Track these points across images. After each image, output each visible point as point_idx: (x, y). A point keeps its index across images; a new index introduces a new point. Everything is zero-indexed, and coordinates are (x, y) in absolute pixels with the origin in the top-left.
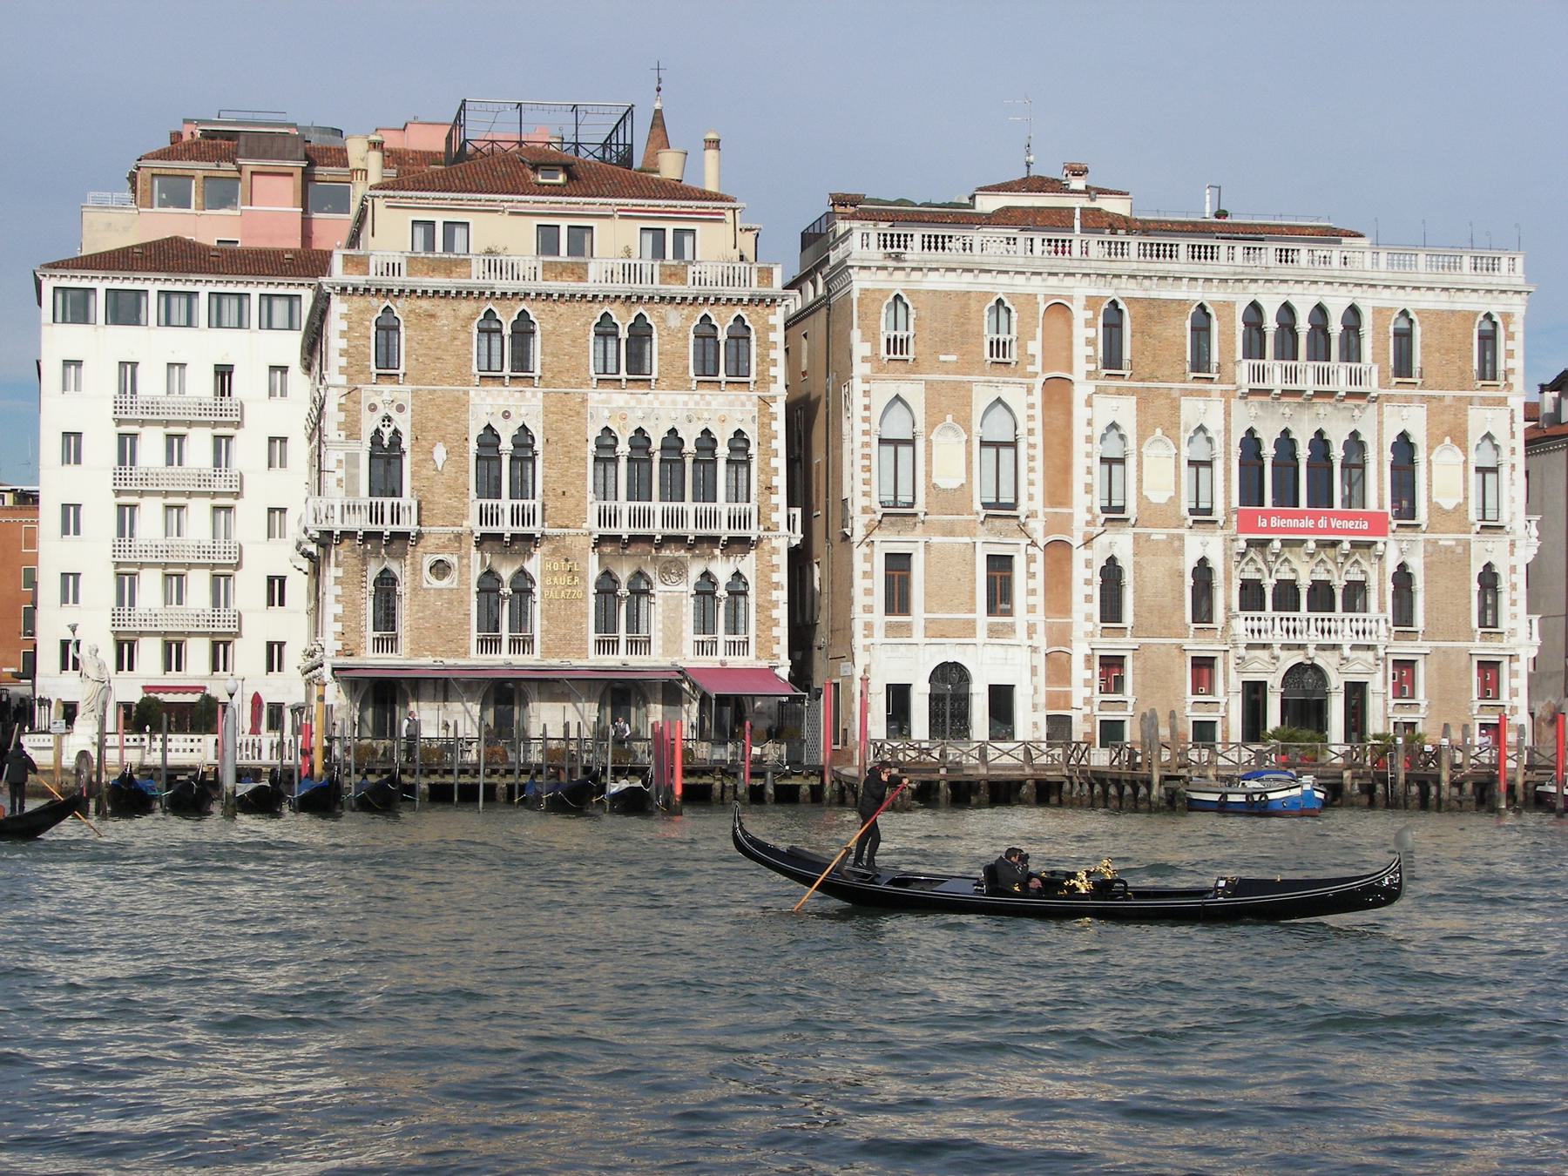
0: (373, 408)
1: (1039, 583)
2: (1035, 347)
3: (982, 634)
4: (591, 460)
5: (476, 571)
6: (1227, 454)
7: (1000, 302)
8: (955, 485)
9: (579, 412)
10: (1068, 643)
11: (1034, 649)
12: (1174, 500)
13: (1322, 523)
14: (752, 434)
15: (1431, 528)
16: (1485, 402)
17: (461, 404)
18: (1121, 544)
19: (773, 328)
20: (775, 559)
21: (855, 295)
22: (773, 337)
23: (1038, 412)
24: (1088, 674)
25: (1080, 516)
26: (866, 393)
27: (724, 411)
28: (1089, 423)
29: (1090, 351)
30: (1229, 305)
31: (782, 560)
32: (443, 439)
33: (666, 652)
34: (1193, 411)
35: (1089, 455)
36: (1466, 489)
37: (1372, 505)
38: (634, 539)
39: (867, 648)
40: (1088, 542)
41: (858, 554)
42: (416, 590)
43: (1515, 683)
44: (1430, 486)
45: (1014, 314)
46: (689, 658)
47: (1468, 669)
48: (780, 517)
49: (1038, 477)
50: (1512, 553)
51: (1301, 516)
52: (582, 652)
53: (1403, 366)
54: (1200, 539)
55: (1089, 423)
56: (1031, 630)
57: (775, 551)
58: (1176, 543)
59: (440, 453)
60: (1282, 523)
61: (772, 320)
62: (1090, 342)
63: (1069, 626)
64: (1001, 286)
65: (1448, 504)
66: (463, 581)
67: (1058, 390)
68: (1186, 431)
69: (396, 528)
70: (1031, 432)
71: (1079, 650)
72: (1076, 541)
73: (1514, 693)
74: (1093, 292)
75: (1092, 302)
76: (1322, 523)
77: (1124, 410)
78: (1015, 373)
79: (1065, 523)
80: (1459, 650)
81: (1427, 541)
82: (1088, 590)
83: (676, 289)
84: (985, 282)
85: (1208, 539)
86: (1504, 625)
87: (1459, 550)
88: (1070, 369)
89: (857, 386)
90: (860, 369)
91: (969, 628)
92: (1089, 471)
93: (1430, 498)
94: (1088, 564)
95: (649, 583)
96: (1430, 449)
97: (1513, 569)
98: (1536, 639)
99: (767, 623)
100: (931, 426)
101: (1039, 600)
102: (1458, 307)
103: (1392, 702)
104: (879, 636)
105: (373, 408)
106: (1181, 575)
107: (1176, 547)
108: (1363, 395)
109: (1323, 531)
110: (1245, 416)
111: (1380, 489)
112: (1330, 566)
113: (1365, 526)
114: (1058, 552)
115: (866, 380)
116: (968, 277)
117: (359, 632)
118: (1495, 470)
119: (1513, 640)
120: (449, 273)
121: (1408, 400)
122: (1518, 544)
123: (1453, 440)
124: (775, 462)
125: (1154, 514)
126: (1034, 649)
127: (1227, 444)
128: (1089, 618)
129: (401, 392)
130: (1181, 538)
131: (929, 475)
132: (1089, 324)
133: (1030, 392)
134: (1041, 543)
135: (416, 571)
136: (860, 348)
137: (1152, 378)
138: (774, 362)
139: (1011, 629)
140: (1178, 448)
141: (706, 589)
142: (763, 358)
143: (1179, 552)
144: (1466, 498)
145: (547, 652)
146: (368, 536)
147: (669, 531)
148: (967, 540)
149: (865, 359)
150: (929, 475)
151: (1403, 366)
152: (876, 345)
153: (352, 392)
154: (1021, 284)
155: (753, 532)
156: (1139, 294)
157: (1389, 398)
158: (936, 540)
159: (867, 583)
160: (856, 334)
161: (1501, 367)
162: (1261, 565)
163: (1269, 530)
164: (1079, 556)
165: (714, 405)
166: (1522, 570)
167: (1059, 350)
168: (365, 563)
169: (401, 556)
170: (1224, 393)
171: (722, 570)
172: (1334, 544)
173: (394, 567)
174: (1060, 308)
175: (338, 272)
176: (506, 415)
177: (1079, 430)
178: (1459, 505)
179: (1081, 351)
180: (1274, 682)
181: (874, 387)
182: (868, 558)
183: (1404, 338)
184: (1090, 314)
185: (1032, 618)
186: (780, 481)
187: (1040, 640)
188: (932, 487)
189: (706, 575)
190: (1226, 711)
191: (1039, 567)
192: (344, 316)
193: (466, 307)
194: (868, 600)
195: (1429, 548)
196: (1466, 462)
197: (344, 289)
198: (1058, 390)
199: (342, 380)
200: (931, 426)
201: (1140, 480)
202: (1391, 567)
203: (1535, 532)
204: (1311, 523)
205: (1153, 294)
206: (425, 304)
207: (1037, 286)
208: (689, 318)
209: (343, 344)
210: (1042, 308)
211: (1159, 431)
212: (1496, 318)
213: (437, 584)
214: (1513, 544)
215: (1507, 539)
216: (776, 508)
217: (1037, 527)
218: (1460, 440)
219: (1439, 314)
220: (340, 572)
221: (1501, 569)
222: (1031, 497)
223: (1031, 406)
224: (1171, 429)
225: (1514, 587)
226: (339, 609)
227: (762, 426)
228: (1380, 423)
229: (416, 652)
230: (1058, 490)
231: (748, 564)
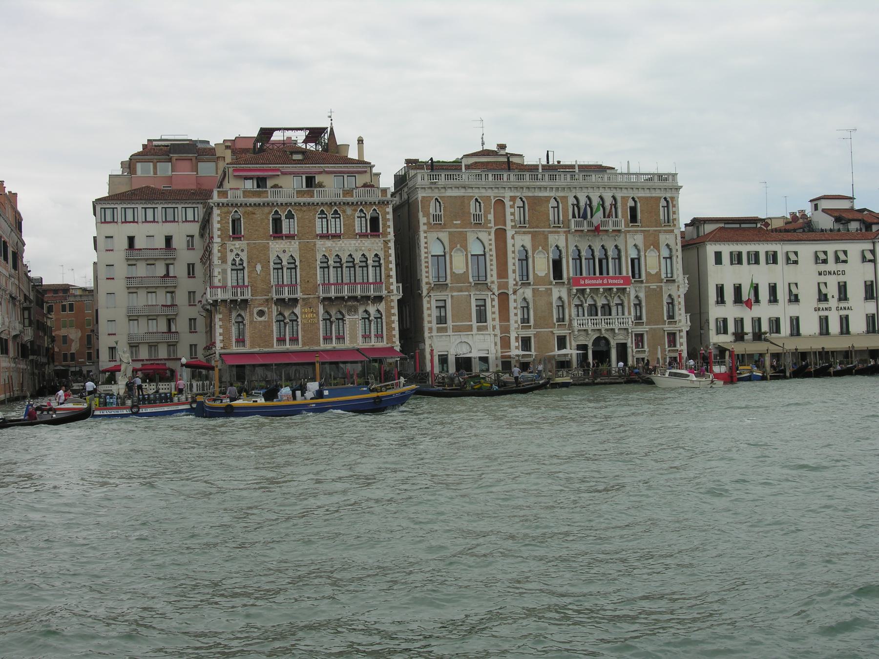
0: (231, 251)
1: (496, 309)
2: (491, 217)
3: (475, 331)
4: (318, 268)
5: (275, 313)
6: (567, 255)
7: (476, 200)
8: (461, 272)
9: (313, 249)
10: (509, 332)
11: (495, 335)
12: (548, 274)
13: (605, 281)
14: (382, 255)
15: (647, 282)
16: (666, 232)
17: (266, 248)
18: (528, 293)
19: (388, 213)
20: (392, 304)
21: (420, 199)
22: (388, 217)
23: (493, 242)
24: (517, 344)
25: (511, 282)
26: (426, 237)
27: (372, 246)
28: (513, 246)
29: (512, 217)
30: (566, 198)
31: (395, 304)
32: (260, 262)
33: (351, 342)
34: (553, 239)
35: (514, 258)
36: (660, 266)
37: (624, 274)
38: (336, 298)
39: (430, 338)
40: (515, 292)
41: (425, 301)
42: (252, 322)
44: (646, 265)
45: (482, 205)
46: (360, 344)
48: (394, 287)
49: (494, 267)
51: (597, 279)
52: (318, 344)
53: (634, 218)
55: (513, 246)
56: (494, 328)
57: (392, 301)
59: (259, 268)
60: (590, 282)
61: (387, 210)
62: (513, 214)
63: (509, 326)
64: (476, 193)
65: (653, 272)
66: (270, 318)
67: (501, 235)
69: (242, 298)
70: (491, 250)
71: (513, 335)
72: (510, 292)
73: (681, 344)
74: (512, 194)
75: (513, 199)
76: (605, 281)
77: (527, 240)
78: (483, 227)
79: (505, 285)
82: (515, 311)
83: (349, 199)
84: (469, 193)
86: (677, 318)
88: (505, 225)
89: (422, 235)
90: (423, 228)
91: (470, 328)
92: (514, 265)
94: (515, 301)
95: (344, 316)
97: (679, 296)
98: (689, 323)
99: (390, 329)
100: (451, 249)
101: (497, 316)
102: (654, 195)
103: (635, 350)
104: (434, 333)
105: (231, 251)
106: (552, 304)
107: (549, 292)
108: (619, 231)
110: (573, 241)
111: (627, 267)
112: (609, 298)
114: (504, 298)
115: (425, 232)
116: (463, 190)
117: (230, 339)
118: (671, 258)
119: (681, 324)
120: (259, 196)
121: (636, 232)
124: (391, 266)
125: (539, 281)
126: (495, 335)
127: (567, 252)
128: (516, 322)
129: (243, 244)
130: (551, 289)
131: (451, 268)
132: (512, 207)
133: (489, 235)
134: (497, 294)
135: (251, 315)
136: (423, 220)
137: (538, 227)
138: (389, 227)
139: (486, 328)
141: (367, 318)
142: (384, 225)
143: (551, 294)
145: (304, 344)
146: (232, 301)
147: (350, 295)
148: (467, 293)
149: (424, 224)
150: (451, 268)
151: (634, 218)
152: (428, 219)
153: (223, 245)
154: (484, 193)
155: (384, 293)
156: (530, 194)
157: (629, 232)
158: (455, 294)
159: (429, 312)
160: (421, 214)
161: (671, 218)
162: (582, 298)
163: (585, 285)
164: (512, 298)
165: (366, 244)
166: (682, 296)
167: (501, 218)
168: (231, 312)
169: (245, 309)
170: (565, 232)
171: (372, 309)
172: (610, 289)
173: (243, 314)
174: (500, 202)
175: (216, 197)
176: (284, 251)
177: (510, 248)
179: (509, 217)
181: (429, 235)
182: (429, 302)
183: (633, 210)
184: (512, 203)
185: (494, 323)
186: (393, 273)
187: (498, 331)
188: (452, 273)
189: (366, 311)
191: (496, 303)
192: (218, 215)
193: (267, 210)
194: (429, 319)
197: (218, 204)
198: (501, 235)
199: (219, 240)
200: (451, 249)
202: (632, 297)
203: (686, 281)
204: (601, 282)
205: (536, 194)
206: (250, 209)
207: (490, 193)
208: (356, 210)
209: (219, 226)
210: (493, 201)
212: (668, 199)
213: (260, 319)
215: (676, 284)
216: (392, 284)
217: (495, 287)
218: (657, 247)
219: (646, 198)
220: (221, 316)
221: (675, 297)
222: (492, 276)
223: (490, 240)
224: (545, 247)
225: (679, 303)
226: (221, 331)
227: (385, 252)
228: (626, 242)
229: (252, 346)
230: (502, 272)
231: (382, 307)
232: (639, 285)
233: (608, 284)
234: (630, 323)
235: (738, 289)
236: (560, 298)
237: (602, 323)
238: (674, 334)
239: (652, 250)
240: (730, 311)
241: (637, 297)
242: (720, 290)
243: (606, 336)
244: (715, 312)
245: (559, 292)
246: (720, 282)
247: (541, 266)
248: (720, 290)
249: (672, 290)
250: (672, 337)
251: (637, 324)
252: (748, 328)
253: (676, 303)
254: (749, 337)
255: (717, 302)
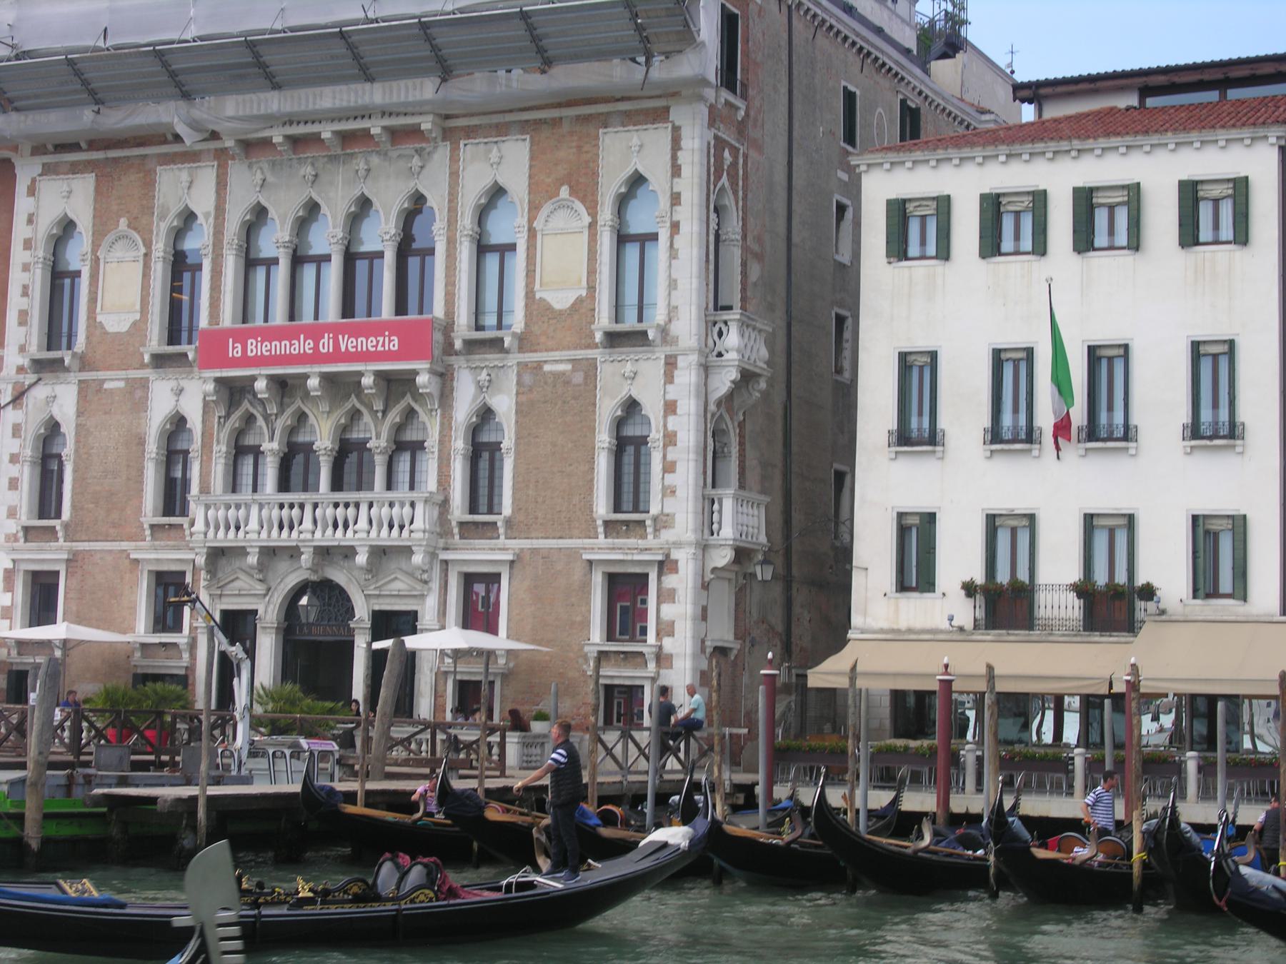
12: (138, 328)
13: (326, 345)
18: (62, 399)
36: (592, 272)
43: (668, 611)
47: (586, 587)
50: (669, 378)
54: (173, 384)
55: (30, 221)
58: (139, 393)
60: (265, 349)
68: (162, 217)
73: (666, 629)
76: (326, 345)
80: (573, 554)
81: (522, 366)
85: (184, 383)
87: (578, 378)
92: (25, 292)
93: (530, 294)
96: (534, 208)
97: (670, 408)
106: (141, 442)
107: (137, 395)
109: (328, 358)
113: (394, 345)
119: (667, 536)
122: (681, 362)
123: (573, 192)
130: (144, 384)
140: (148, 244)
144: (591, 288)
163: (245, 361)
166: (689, 407)
178: (579, 301)
180: (269, 613)
190: (193, 656)
195: (527, 379)
196: (592, 226)
201: (93, 300)
202: (463, 410)
211: (123, 222)
214: (671, 363)
215: (660, 353)
221: (652, 407)
225: (670, 439)
228: (454, 175)
232: (493, 358)
233: (337, 356)
234: (423, 519)
235: (1009, 367)
236: (178, 423)
237: (316, 521)
238: (640, 581)
239: (562, 206)
240: (962, 486)
241: (486, 414)
242: (918, 373)
243: (339, 576)
244: (884, 485)
245: (187, 395)
246: (920, 343)
247: (122, 293)
248: (918, 373)
249: (640, 377)
250: (626, 592)
251: (467, 529)
252: (1058, 567)
253: (655, 435)
254: (1057, 600)
255: (903, 438)
